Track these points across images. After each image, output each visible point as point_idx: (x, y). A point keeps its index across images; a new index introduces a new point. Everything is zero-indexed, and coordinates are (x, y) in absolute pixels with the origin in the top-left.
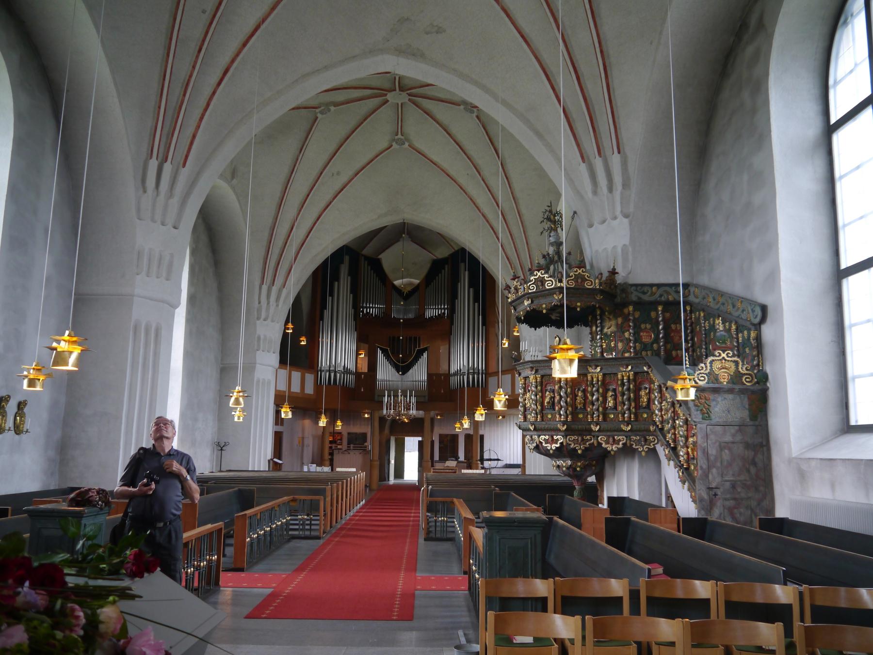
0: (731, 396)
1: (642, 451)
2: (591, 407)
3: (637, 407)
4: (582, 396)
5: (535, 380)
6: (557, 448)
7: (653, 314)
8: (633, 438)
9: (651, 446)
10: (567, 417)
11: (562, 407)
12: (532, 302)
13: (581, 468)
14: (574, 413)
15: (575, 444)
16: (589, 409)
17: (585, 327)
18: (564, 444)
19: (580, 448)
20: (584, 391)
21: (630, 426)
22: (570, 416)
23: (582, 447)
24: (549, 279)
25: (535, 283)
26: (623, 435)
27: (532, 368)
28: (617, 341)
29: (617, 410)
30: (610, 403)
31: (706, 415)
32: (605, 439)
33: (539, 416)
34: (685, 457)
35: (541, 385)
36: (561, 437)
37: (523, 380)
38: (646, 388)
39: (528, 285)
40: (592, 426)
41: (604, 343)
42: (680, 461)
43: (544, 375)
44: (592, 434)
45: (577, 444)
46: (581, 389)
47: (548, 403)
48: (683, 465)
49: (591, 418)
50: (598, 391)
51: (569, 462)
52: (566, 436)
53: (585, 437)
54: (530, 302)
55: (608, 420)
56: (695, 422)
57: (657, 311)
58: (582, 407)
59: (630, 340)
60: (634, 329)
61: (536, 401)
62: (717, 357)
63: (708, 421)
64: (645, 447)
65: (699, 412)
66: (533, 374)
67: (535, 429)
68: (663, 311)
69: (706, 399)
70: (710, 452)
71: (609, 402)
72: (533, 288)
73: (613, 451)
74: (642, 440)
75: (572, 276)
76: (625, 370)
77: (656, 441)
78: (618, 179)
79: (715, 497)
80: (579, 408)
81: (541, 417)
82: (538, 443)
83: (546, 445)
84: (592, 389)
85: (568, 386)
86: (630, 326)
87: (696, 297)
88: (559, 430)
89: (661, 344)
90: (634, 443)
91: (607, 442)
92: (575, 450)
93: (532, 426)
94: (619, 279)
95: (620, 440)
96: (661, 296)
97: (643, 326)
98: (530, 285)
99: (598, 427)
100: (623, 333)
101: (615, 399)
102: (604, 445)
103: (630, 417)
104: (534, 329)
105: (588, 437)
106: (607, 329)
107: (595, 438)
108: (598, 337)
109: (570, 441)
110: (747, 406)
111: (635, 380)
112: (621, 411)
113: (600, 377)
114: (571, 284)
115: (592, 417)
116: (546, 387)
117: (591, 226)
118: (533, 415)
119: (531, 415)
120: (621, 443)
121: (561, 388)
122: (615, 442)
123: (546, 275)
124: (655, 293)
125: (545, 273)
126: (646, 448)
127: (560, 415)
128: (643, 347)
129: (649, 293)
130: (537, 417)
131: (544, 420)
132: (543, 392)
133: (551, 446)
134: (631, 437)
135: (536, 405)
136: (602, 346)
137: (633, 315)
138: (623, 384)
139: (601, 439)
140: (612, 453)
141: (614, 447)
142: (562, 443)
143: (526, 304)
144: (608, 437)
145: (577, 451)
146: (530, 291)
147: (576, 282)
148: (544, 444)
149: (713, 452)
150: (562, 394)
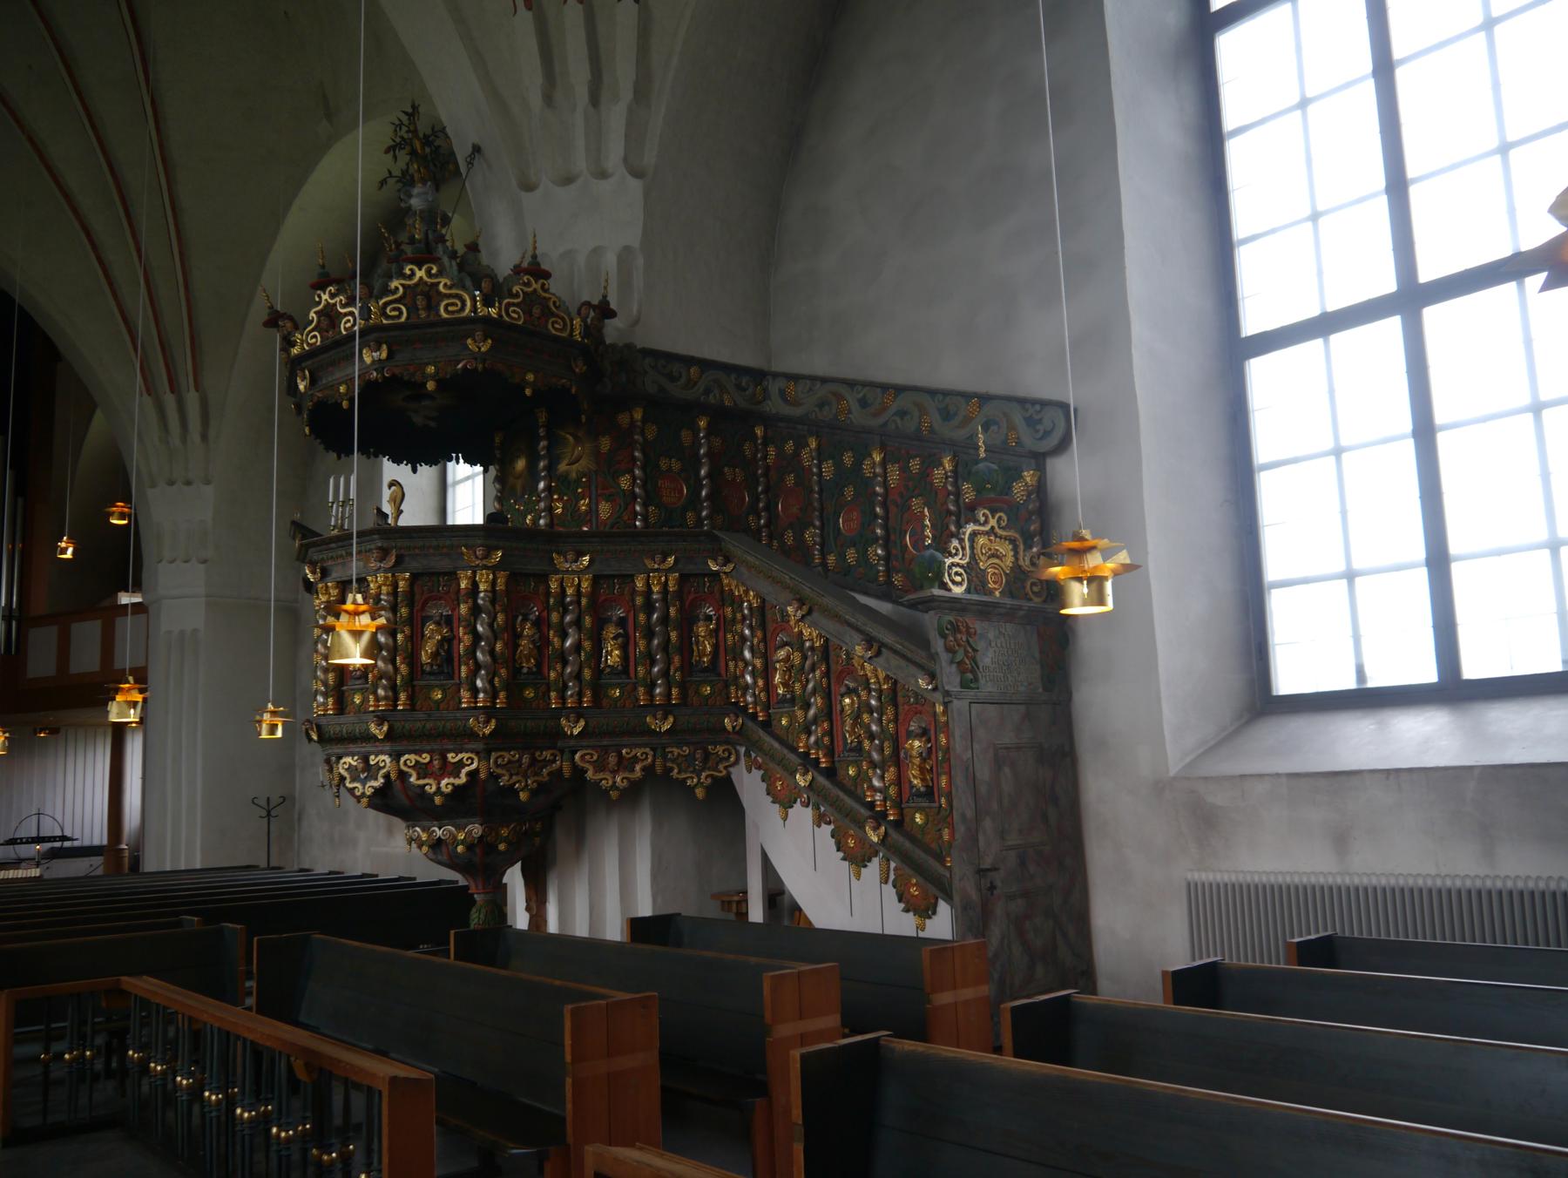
0: (1009, 628)
1: (696, 785)
2: (559, 666)
3: (688, 667)
4: (537, 636)
5: (390, 588)
6: (456, 788)
7: (686, 435)
8: (671, 752)
9: (721, 772)
10: (494, 696)
11: (478, 666)
12: (390, 355)
13: (509, 843)
14: (514, 686)
15: (511, 775)
16: (553, 675)
17: (468, 466)
18: (482, 776)
19: (527, 785)
20: (537, 624)
21: (671, 719)
22: (502, 695)
23: (529, 782)
24: (453, 291)
25: (402, 301)
26: (645, 746)
27: (384, 553)
28: (594, 496)
29: (629, 678)
30: (613, 657)
31: (970, 676)
32: (595, 758)
33: (403, 696)
34: (892, 791)
35: (411, 605)
36: (473, 756)
37: (334, 592)
38: (708, 618)
39: (381, 303)
40: (563, 721)
41: (557, 500)
42: (872, 805)
43: (422, 574)
44: (560, 744)
45: (517, 774)
46: (532, 617)
47: (435, 655)
48: (884, 815)
49: (556, 698)
50: (578, 623)
51: (476, 829)
52: (489, 752)
53: (537, 754)
54: (384, 355)
55: (605, 702)
56: (947, 694)
57: (696, 431)
58: (534, 669)
59: (634, 497)
60: (643, 468)
61: (394, 651)
62: (980, 524)
63: (972, 693)
64: (704, 775)
65: (954, 667)
66: (386, 571)
67: (389, 736)
68: (710, 432)
69: (969, 634)
70: (978, 775)
71: (609, 653)
72: (396, 313)
73: (617, 788)
74: (697, 756)
75: (517, 296)
76: (656, 566)
77: (732, 759)
78: (623, 72)
79: (992, 894)
80: (525, 670)
81: (408, 698)
82: (393, 776)
83: (421, 782)
84: (562, 617)
85: (498, 608)
86: (634, 459)
87: (796, 403)
88: (472, 735)
89: (704, 513)
90: (675, 766)
91: (600, 766)
92: (511, 791)
93: (380, 724)
94: (613, 330)
95: (635, 759)
96: (707, 392)
97: (663, 464)
98: (386, 304)
99: (582, 723)
100: (616, 476)
101: (624, 648)
102: (590, 775)
103: (668, 695)
104: (335, 455)
105: (547, 754)
106: (567, 465)
107: (565, 757)
108: (542, 485)
109: (498, 766)
110: (1037, 655)
111: (680, 594)
112: (644, 679)
113: (585, 585)
114: (515, 316)
115: (563, 698)
116: (423, 608)
117: (529, 187)
118: (381, 692)
119: (375, 693)
120: (638, 768)
121: (476, 611)
122: (625, 764)
123: (443, 281)
124: (696, 383)
125: (440, 273)
126: (706, 777)
127: (475, 691)
128: (663, 515)
129: (683, 380)
130: (396, 699)
131: (418, 707)
132: (416, 625)
133: (439, 784)
134: (667, 750)
135: (393, 662)
136: (550, 509)
137: (643, 434)
138: (649, 607)
139: (582, 757)
140: (614, 794)
141: (618, 779)
142: (470, 774)
143: (368, 360)
144: (605, 751)
145: (516, 793)
146: (384, 322)
147: (528, 313)
148: (412, 779)
149: (984, 773)
150: (480, 628)
